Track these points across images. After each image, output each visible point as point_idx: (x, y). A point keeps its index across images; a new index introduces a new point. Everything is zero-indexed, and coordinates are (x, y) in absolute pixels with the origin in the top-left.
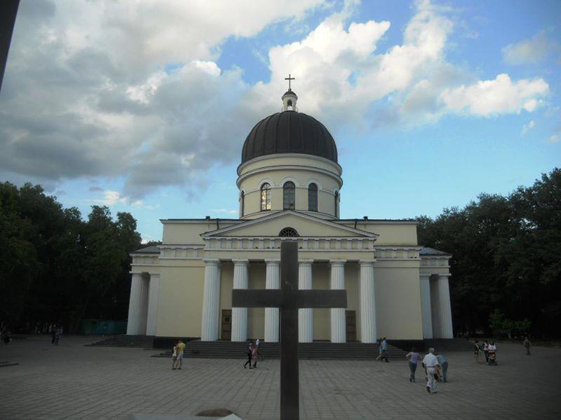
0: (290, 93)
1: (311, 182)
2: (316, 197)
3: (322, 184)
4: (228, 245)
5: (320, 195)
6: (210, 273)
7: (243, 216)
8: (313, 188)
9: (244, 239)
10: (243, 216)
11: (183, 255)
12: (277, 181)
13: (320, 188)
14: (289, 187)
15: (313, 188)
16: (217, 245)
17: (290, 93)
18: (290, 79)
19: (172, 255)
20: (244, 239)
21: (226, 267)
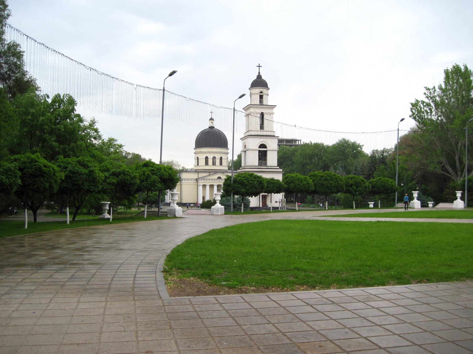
0: (212, 119)
1: (221, 156)
2: (222, 161)
3: (224, 157)
4: (205, 181)
5: (223, 160)
6: (201, 188)
7: (198, 164)
8: (221, 159)
9: (209, 179)
10: (198, 164)
11: (189, 181)
12: (210, 157)
13: (223, 158)
14: (214, 158)
15: (221, 158)
16: (203, 181)
17: (212, 119)
18: (211, 113)
19: (186, 181)
20: (209, 179)
21: (204, 186)
